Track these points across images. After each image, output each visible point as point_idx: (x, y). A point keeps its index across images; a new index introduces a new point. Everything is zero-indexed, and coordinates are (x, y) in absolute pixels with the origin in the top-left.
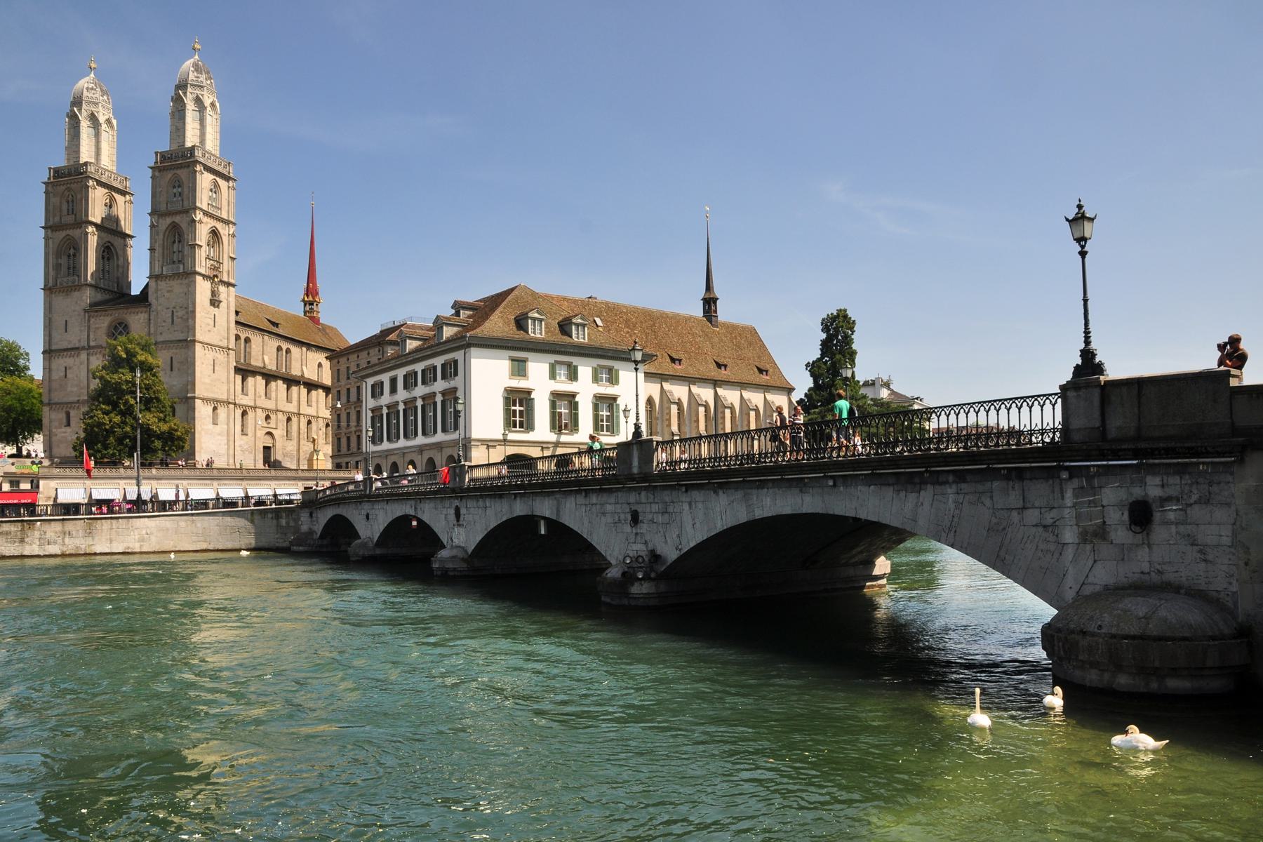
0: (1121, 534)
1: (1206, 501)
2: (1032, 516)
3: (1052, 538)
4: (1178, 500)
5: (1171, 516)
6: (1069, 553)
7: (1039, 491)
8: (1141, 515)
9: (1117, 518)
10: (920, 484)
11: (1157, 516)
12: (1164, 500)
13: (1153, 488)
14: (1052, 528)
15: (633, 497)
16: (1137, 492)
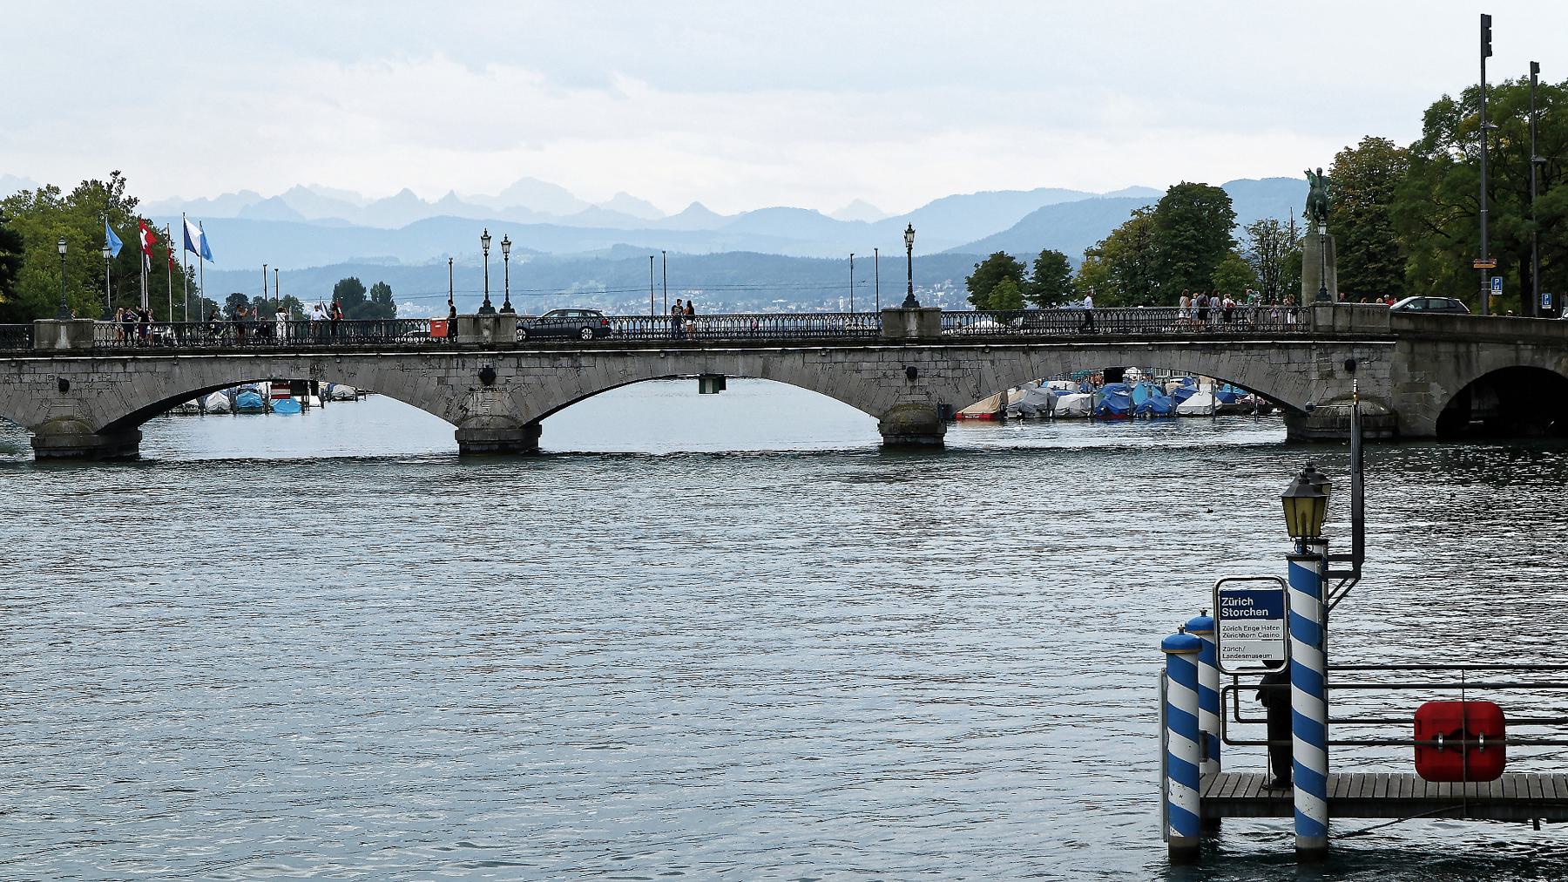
0: (1341, 375)
1: (1379, 360)
2: (1294, 367)
3: (1304, 378)
4: (1367, 360)
5: (1364, 366)
6: (1314, 384)
7: (1297, 355)
8: (1351, 366)
9: (1339, 369)
10: (1221, 349)
11: (1358, 366)
12: (1362, 359)
13: (1357, 354)
14: (1305, 372)
15: (909, 358)
16: (1349, 355)
